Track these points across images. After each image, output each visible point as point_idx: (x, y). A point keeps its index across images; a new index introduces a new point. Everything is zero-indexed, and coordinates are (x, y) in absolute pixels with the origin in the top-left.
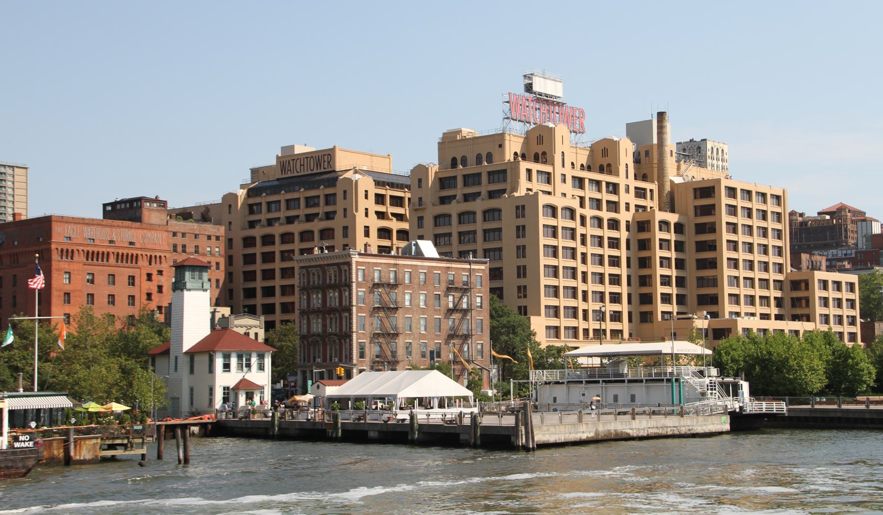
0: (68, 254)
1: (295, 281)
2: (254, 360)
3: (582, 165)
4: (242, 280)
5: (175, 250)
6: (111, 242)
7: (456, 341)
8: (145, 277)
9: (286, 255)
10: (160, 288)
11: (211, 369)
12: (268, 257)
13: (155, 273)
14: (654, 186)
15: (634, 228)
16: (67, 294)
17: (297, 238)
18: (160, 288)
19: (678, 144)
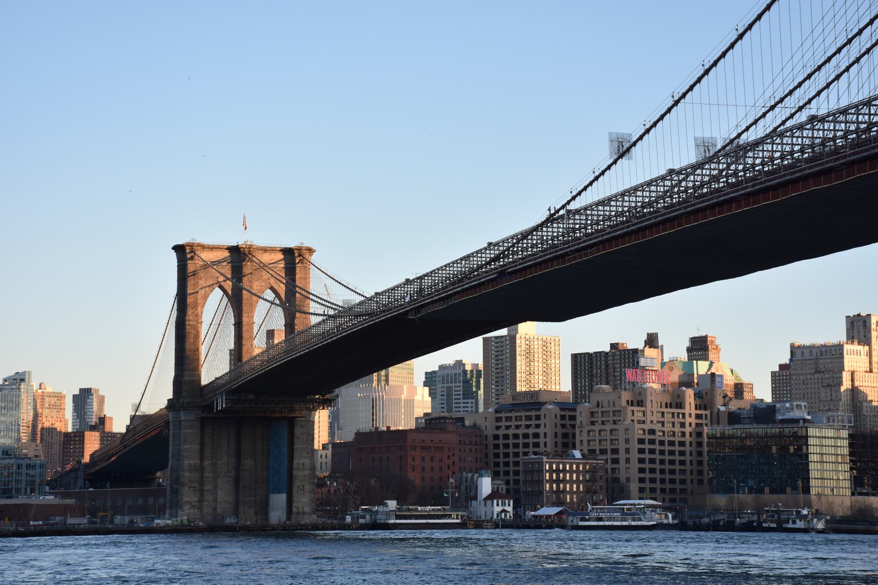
0: (414, 448)
1: (521, 468)
2: (507, 501)
3: (666, 403)
4: (492, 457)
5: (460, 444)
6: (432, 441)
7: (590, 494)
8: (447, 458)
9: (516, 455)
10: (454, 463)
11: (493, 505)
12: (506, 446)
13: (451, 455)
14: (708, 412)
15: (694, 435)
16: (413, 467)
17: (521, 437)
18: (454, 463)
19: (847, 317)
